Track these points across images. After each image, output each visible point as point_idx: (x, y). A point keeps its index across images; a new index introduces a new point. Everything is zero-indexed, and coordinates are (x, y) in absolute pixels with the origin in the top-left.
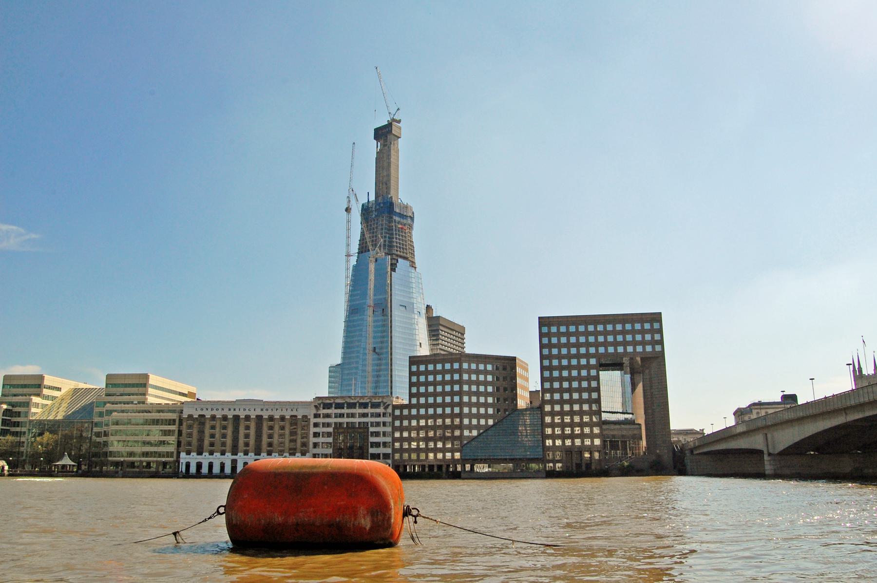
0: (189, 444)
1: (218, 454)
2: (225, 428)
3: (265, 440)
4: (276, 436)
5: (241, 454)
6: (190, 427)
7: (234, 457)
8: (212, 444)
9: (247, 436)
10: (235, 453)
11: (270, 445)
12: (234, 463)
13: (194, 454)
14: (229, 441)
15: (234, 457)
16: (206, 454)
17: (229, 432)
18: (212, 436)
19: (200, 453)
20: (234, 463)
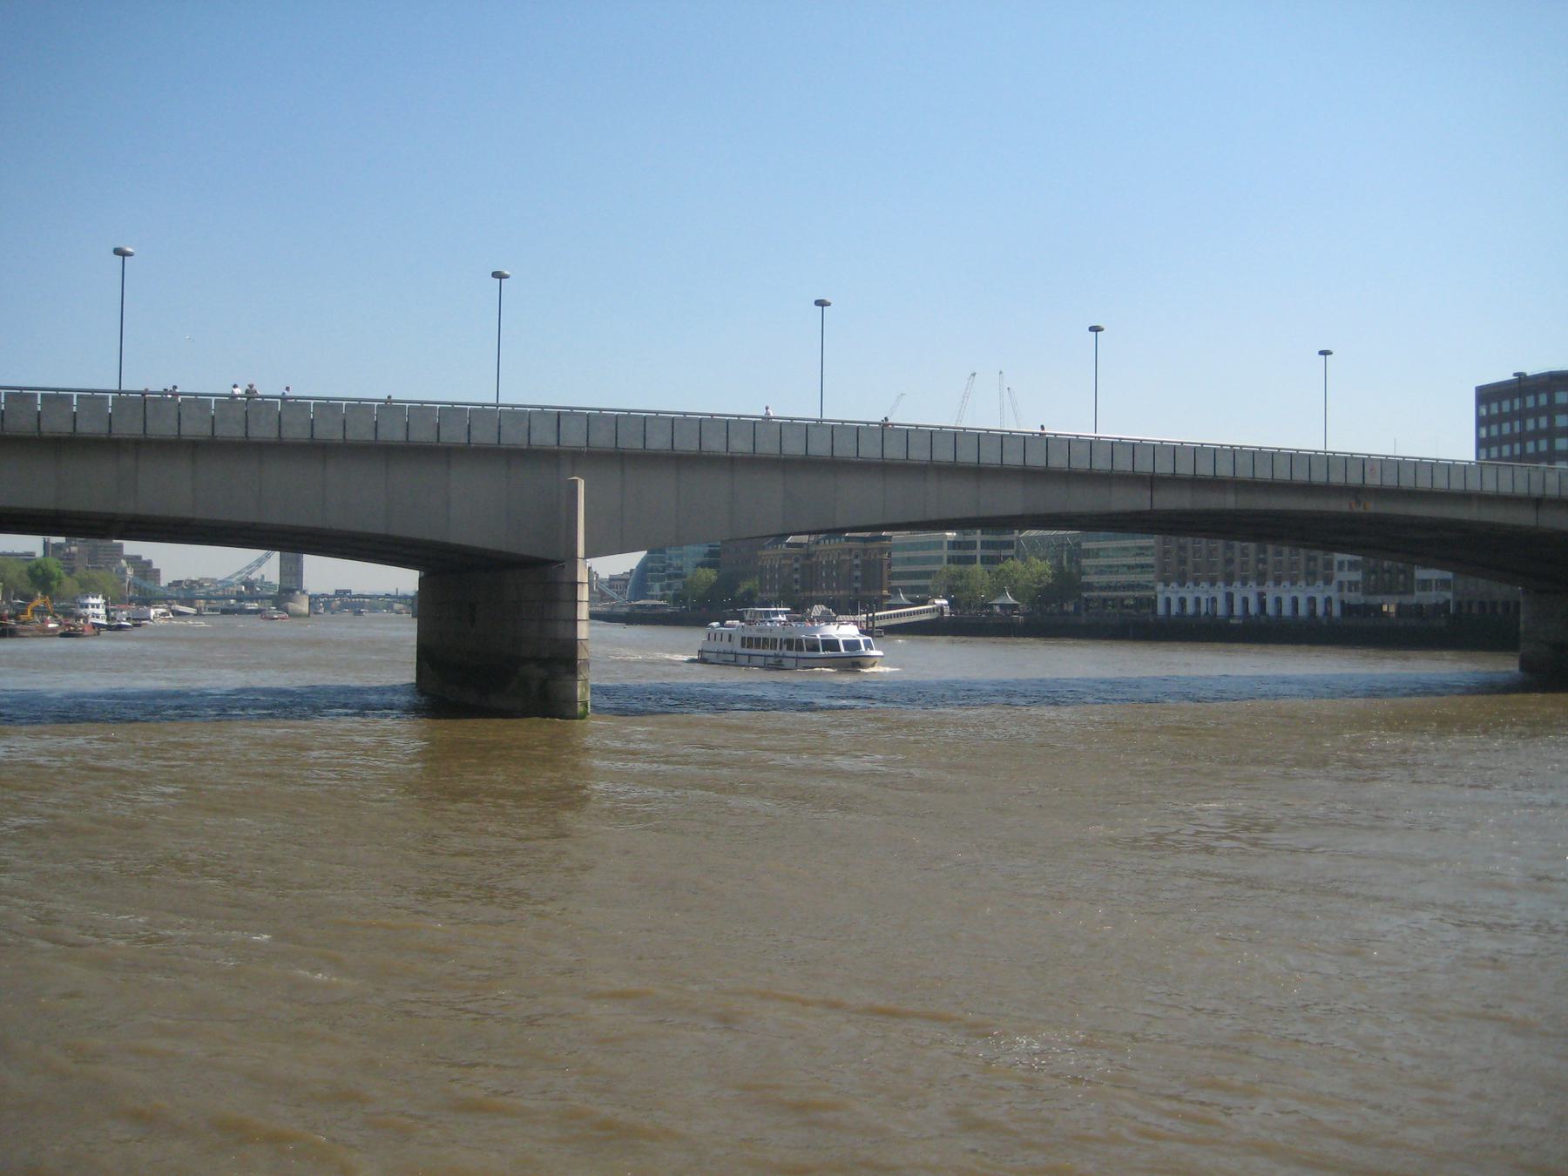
1: (1205, 585)
5: (1237, 584)
7: (1229, 589)
8: (1196, 569)
10: (1229, 583)
12: (1229, 598)
15: (1229, 589)
16: (1190, 584)
20: (1229, 598)
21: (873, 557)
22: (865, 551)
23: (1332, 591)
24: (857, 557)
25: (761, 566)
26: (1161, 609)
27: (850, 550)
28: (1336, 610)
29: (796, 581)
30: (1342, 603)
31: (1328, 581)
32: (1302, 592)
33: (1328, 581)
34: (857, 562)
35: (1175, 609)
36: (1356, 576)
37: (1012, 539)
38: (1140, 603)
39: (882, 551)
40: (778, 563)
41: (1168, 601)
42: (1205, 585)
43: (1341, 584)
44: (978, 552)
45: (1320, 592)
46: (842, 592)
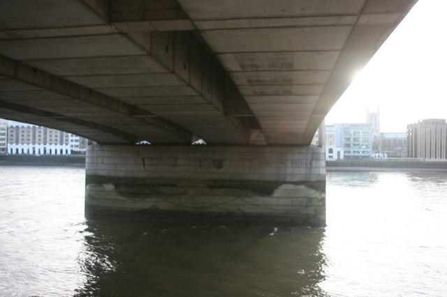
0: (12, 139)
2: (29, 132)
3: (48, 138)
4: (53, 136)
6: (12, 131)
8: (23, 140)
9: (40, 136)
10: (34, 143)
11: (51, 140)
12: (34, 148)
13: (14, 144)
14: (31, 138)
17: (31, 134)
18: (23, 136)
19: (17, 144)
20: (34, 148)
23: (69, 149)
26: (9, 152)
28: (69, 153)
30: (72, 151)
31: (67, 144)
32: (59, 147)
33: (67, 144)
36: (77, 143)
38: (3, 149)
42: (25, 145)
43: (72, 146)
45: (64, 147)
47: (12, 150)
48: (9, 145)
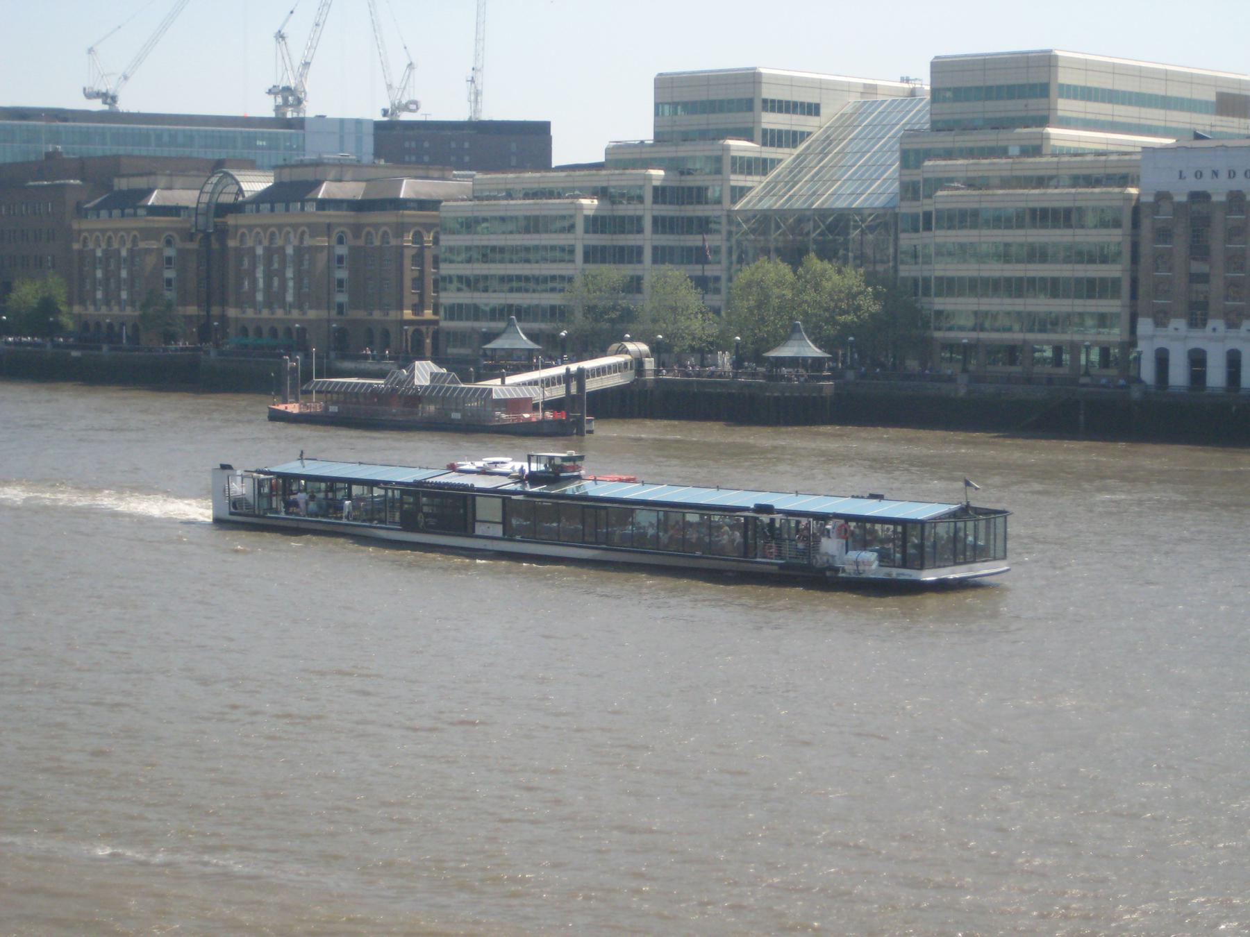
16: (1217, 324)
21: (377, 243)
22: (357, 229)
24: (341, 241)
25: (80, 252)
26: (1148, 372)
27: (329, 227)
29: (169, 282)
34: (342, 250)
35: (1178, 375)
37: (718, 213)
39: (400, 229)
40: (129, 245)
41: (1162, 359)
44: (647, 240)
46: (312, 314)
47: (1162, 359)
48: (1145, 326)
